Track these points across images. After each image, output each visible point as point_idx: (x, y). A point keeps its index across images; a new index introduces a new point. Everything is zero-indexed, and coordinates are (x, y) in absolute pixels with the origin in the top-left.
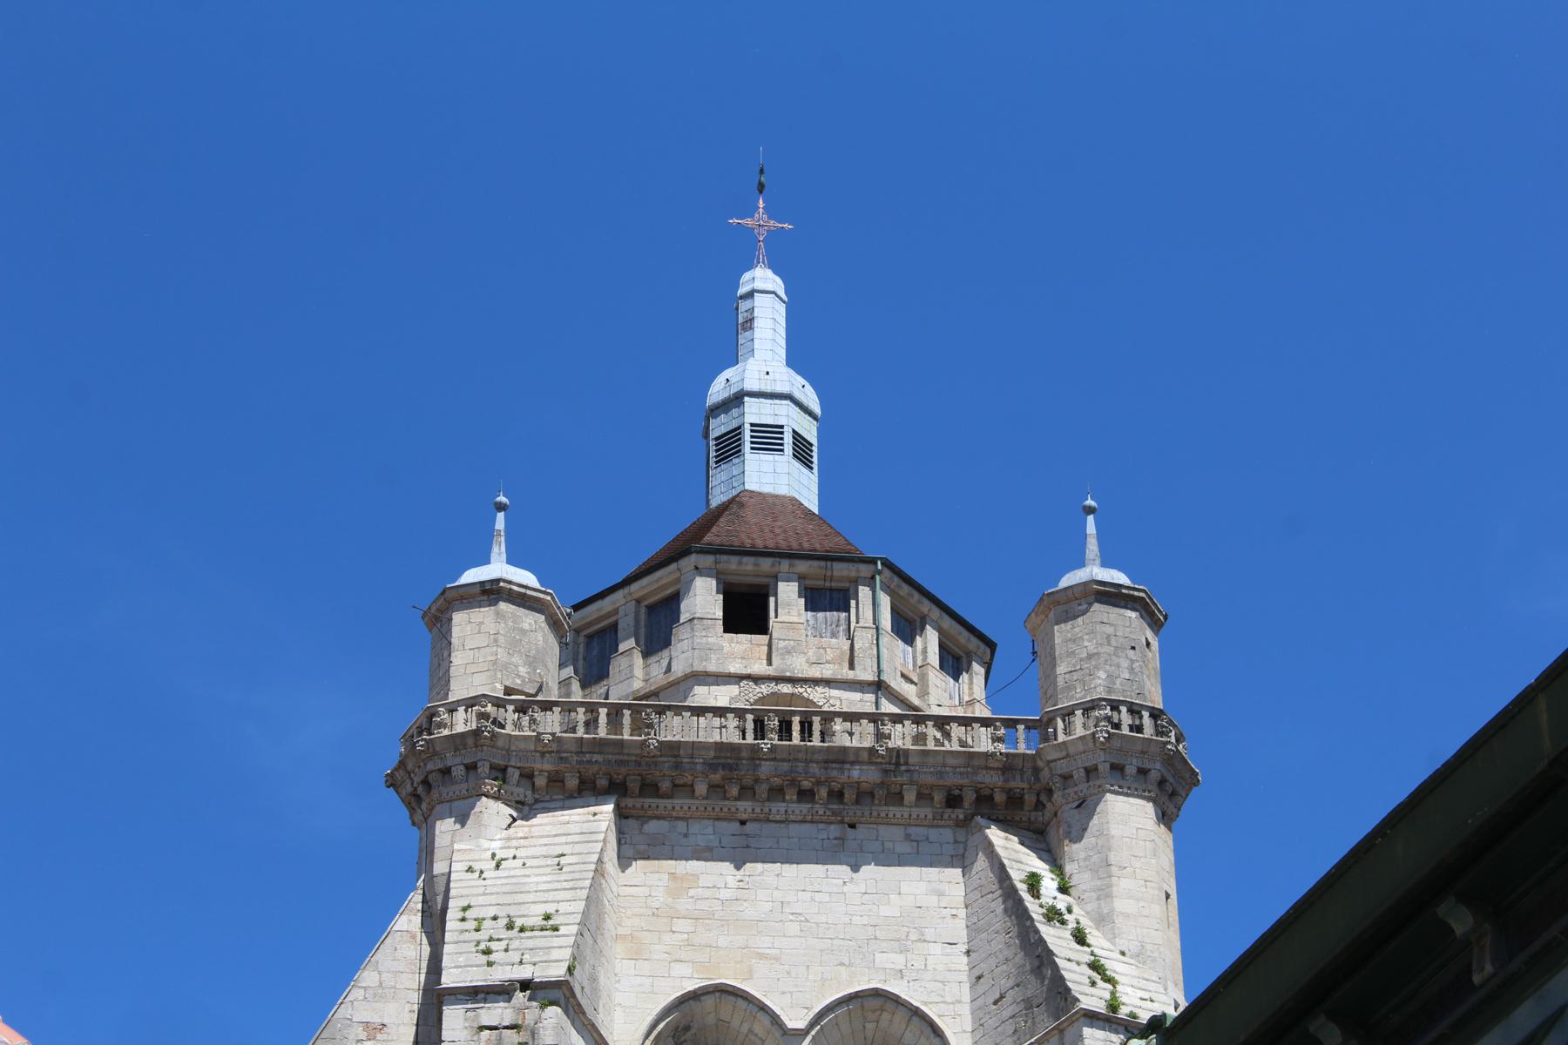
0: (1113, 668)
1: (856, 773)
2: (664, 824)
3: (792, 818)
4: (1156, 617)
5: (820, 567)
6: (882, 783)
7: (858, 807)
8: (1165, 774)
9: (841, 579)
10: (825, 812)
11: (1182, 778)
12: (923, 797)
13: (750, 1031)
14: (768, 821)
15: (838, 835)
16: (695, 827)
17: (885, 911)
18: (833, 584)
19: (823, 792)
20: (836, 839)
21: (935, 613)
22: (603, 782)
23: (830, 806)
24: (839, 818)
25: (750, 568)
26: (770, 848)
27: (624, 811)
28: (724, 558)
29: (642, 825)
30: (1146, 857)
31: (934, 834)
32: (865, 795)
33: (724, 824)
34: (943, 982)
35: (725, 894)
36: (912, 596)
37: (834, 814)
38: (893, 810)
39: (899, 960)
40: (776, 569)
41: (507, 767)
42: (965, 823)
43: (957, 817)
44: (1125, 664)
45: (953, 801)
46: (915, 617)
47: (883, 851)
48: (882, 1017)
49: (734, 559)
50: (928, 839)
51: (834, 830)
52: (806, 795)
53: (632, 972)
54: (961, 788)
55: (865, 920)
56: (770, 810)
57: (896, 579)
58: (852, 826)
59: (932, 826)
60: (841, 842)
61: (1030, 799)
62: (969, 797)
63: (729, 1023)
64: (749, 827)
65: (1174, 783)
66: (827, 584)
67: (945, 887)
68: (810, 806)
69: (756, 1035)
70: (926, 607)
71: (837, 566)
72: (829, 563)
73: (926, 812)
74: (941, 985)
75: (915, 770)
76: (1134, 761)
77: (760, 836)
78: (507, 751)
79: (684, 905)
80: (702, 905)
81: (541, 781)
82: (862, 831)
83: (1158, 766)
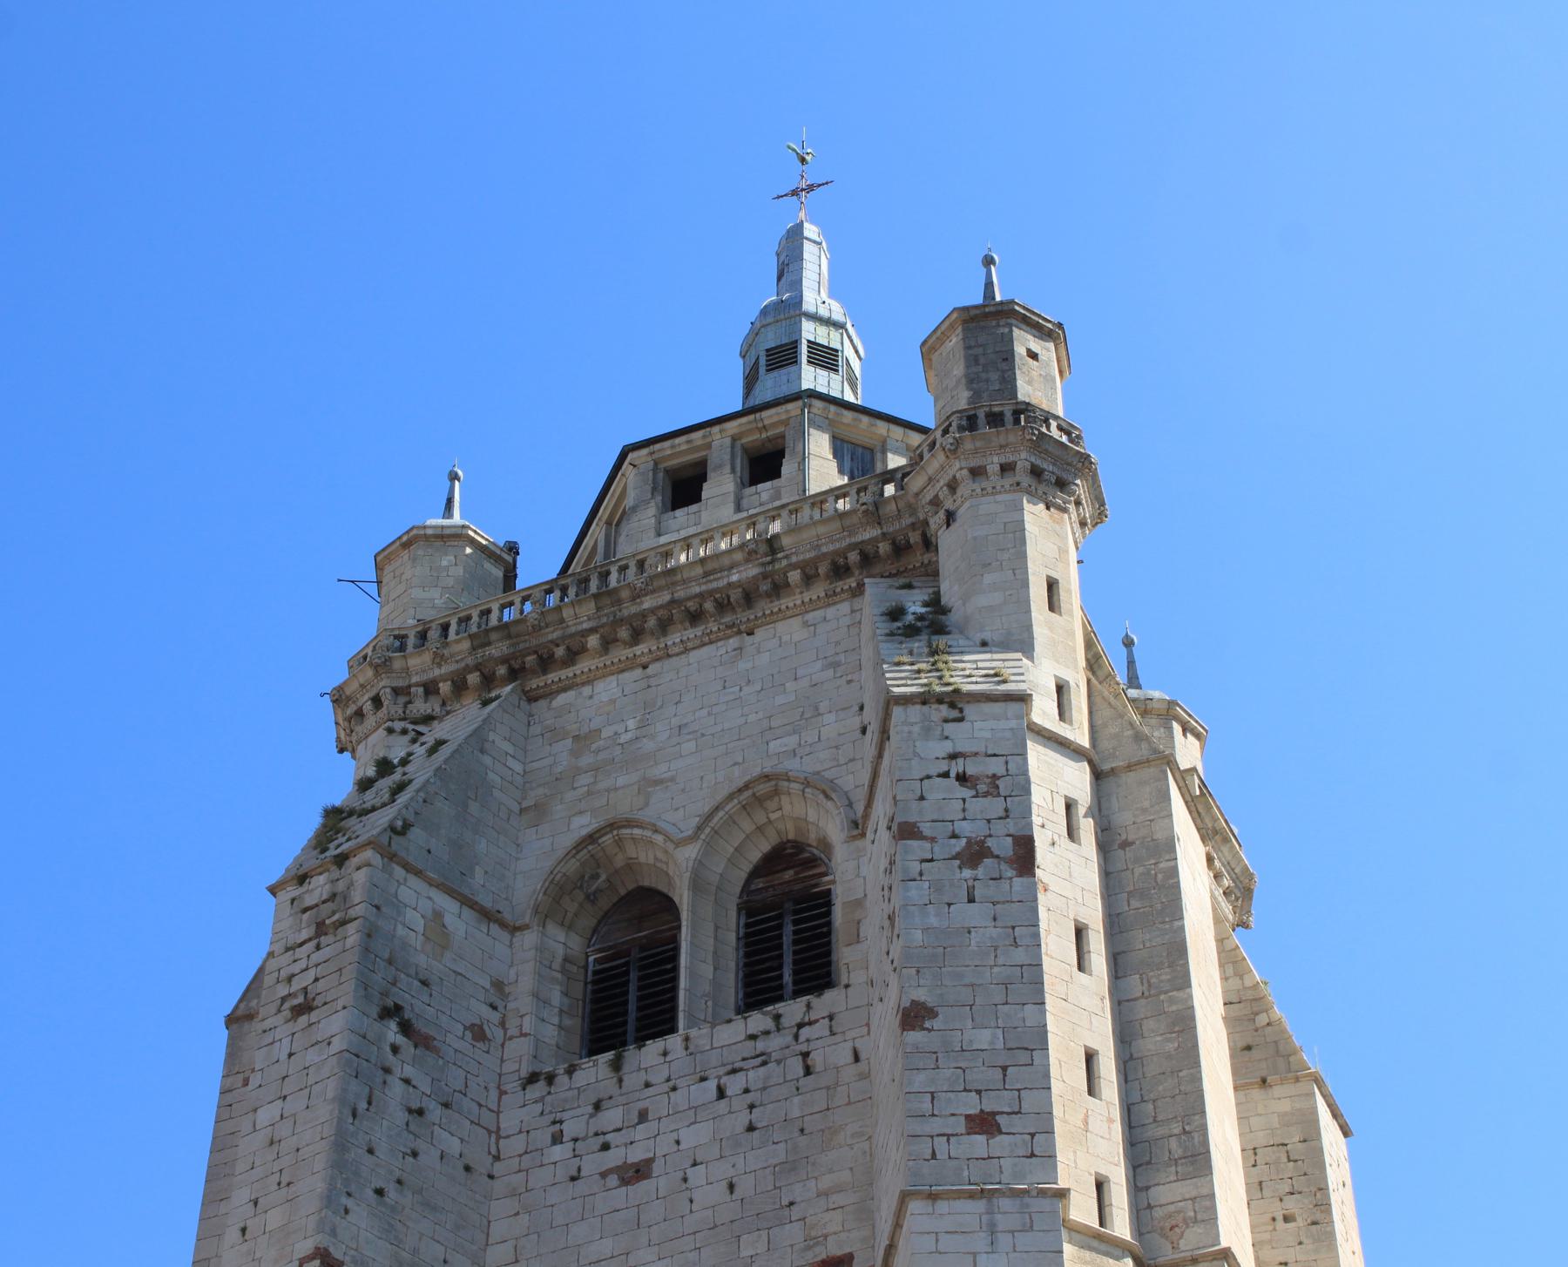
0: (981, 384)
1: (735, 578)
2: (571, 694)
3: (690, 645)
4: (1047, 330)
5: (750, 422)
6: (765, 576)
7: (751, 611)
8: (1038, 462)
9: (774, 425)
10: (719, 629)
11: (1068, 464)
12: (809, 579)
13: (656, 858)
14: (669, 656)
15: (736, 646)
16: (600, 686)
17: (780, 700)
18: (769, 434)
19: (709, 606)
20: (735, 650)
21: (897, 432)
22: (502, 671)
23: (723, 621)
24: (735, 630)
25: (684, 447)
26: (671, 680)
27: (531, 694)
28: (657, 446)
29: (550, 702)
30: (1015, 547)
31: (830, 612)
32: (749, 597)
33: (626, 675)
34: (837, 747)
35: (624, 738)
36: (860, 421)
37: (728, 627)
38: (785, 602)
39: (792, 741)
40: (709, 440)
41: (409, 686)
42: (859, 590)
43: (850, 586)
44: (994, 376)
45: (840, 570)
46: (876, 443)
47: (780, 646)
48: (783, 803)
49: (667, 444)
50: (825, 618)
51: (733, 642)
52: (695, 617)
53: (534, 837)
54: (843, 553)
55: (761, 715)
56: (666, 645)
57: (833, 408)
58: (750, 633)
59: (829, 605)
60: (739, 651)
61: (914, 538)
62: (853, 557)
63: (637, 858)
64: (649, 671)
65: (1056, 470)
66: (764, 436)
67: (842, 657)
68: (703, 627)
69: (661, 861)
70: (882, 427)
71: (765, 414)
72: (758, 415)
73: (819, 590)
74: (834, 750)
75: (792, 554)
76: (996, 459)
77: (661, 673)
78: (407, 673)
79: (586, 760)
80: (602, 756)
81: (445, 688)
82: (760, 634)
83: (1024, 455)
